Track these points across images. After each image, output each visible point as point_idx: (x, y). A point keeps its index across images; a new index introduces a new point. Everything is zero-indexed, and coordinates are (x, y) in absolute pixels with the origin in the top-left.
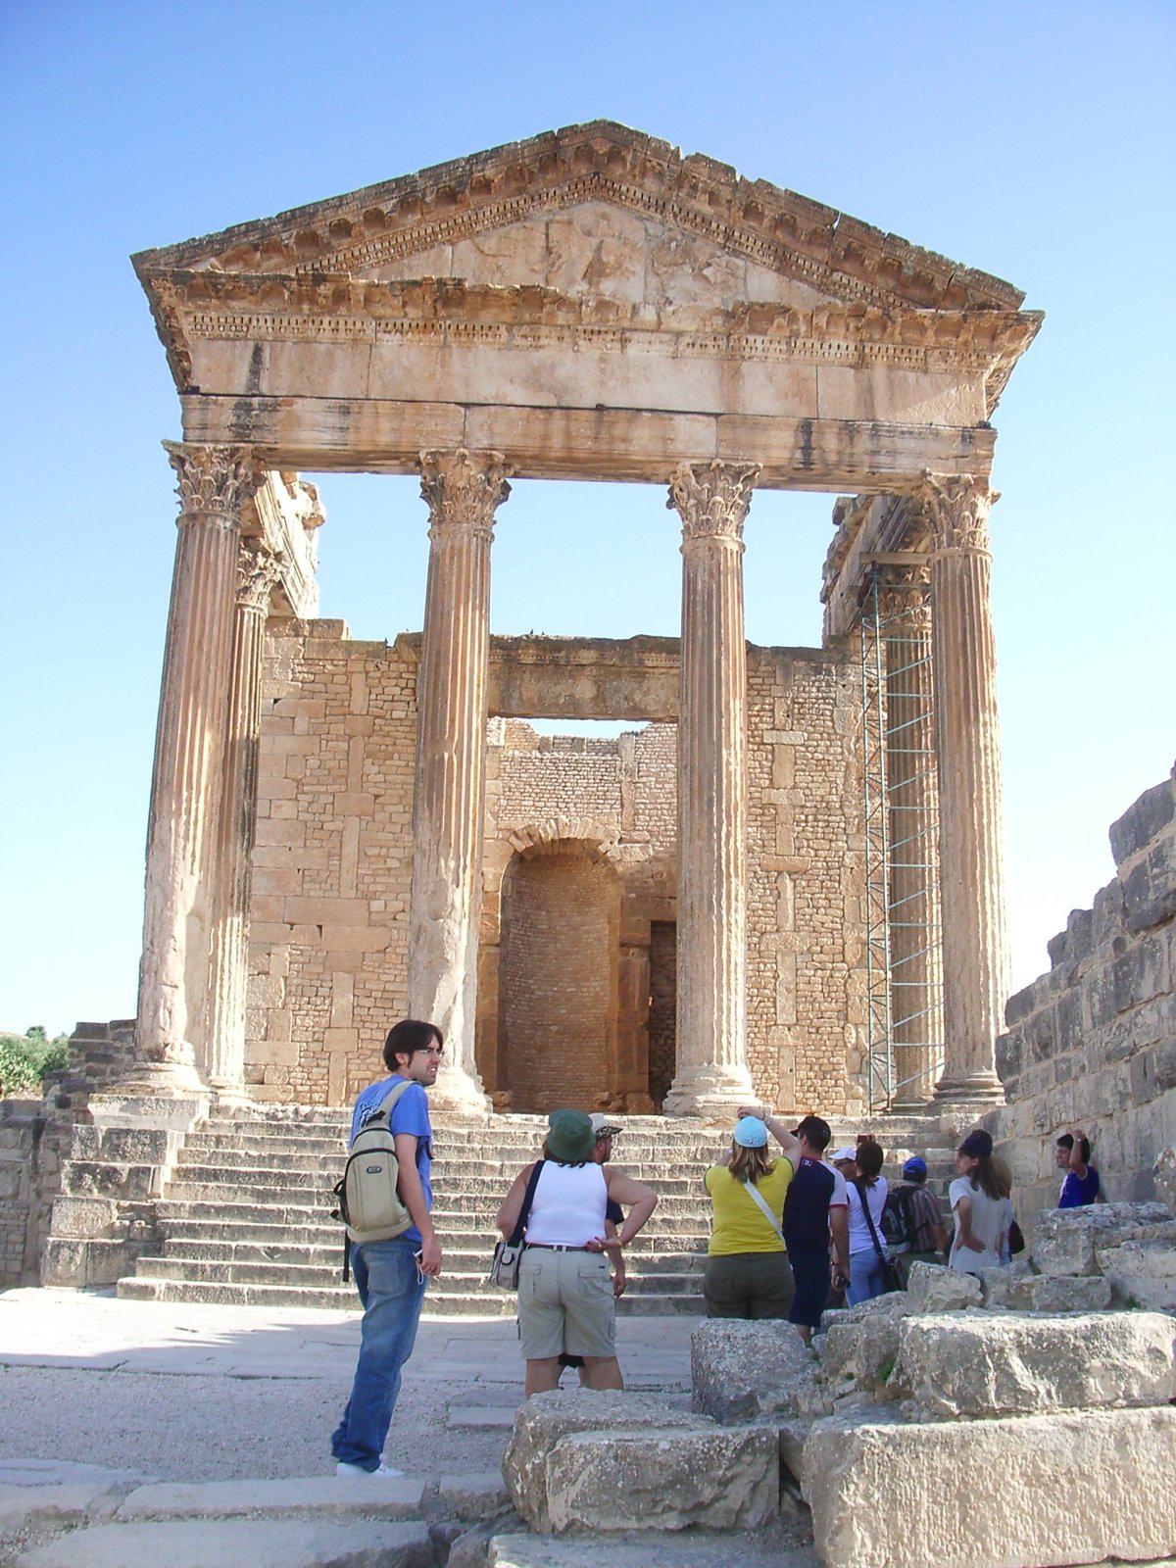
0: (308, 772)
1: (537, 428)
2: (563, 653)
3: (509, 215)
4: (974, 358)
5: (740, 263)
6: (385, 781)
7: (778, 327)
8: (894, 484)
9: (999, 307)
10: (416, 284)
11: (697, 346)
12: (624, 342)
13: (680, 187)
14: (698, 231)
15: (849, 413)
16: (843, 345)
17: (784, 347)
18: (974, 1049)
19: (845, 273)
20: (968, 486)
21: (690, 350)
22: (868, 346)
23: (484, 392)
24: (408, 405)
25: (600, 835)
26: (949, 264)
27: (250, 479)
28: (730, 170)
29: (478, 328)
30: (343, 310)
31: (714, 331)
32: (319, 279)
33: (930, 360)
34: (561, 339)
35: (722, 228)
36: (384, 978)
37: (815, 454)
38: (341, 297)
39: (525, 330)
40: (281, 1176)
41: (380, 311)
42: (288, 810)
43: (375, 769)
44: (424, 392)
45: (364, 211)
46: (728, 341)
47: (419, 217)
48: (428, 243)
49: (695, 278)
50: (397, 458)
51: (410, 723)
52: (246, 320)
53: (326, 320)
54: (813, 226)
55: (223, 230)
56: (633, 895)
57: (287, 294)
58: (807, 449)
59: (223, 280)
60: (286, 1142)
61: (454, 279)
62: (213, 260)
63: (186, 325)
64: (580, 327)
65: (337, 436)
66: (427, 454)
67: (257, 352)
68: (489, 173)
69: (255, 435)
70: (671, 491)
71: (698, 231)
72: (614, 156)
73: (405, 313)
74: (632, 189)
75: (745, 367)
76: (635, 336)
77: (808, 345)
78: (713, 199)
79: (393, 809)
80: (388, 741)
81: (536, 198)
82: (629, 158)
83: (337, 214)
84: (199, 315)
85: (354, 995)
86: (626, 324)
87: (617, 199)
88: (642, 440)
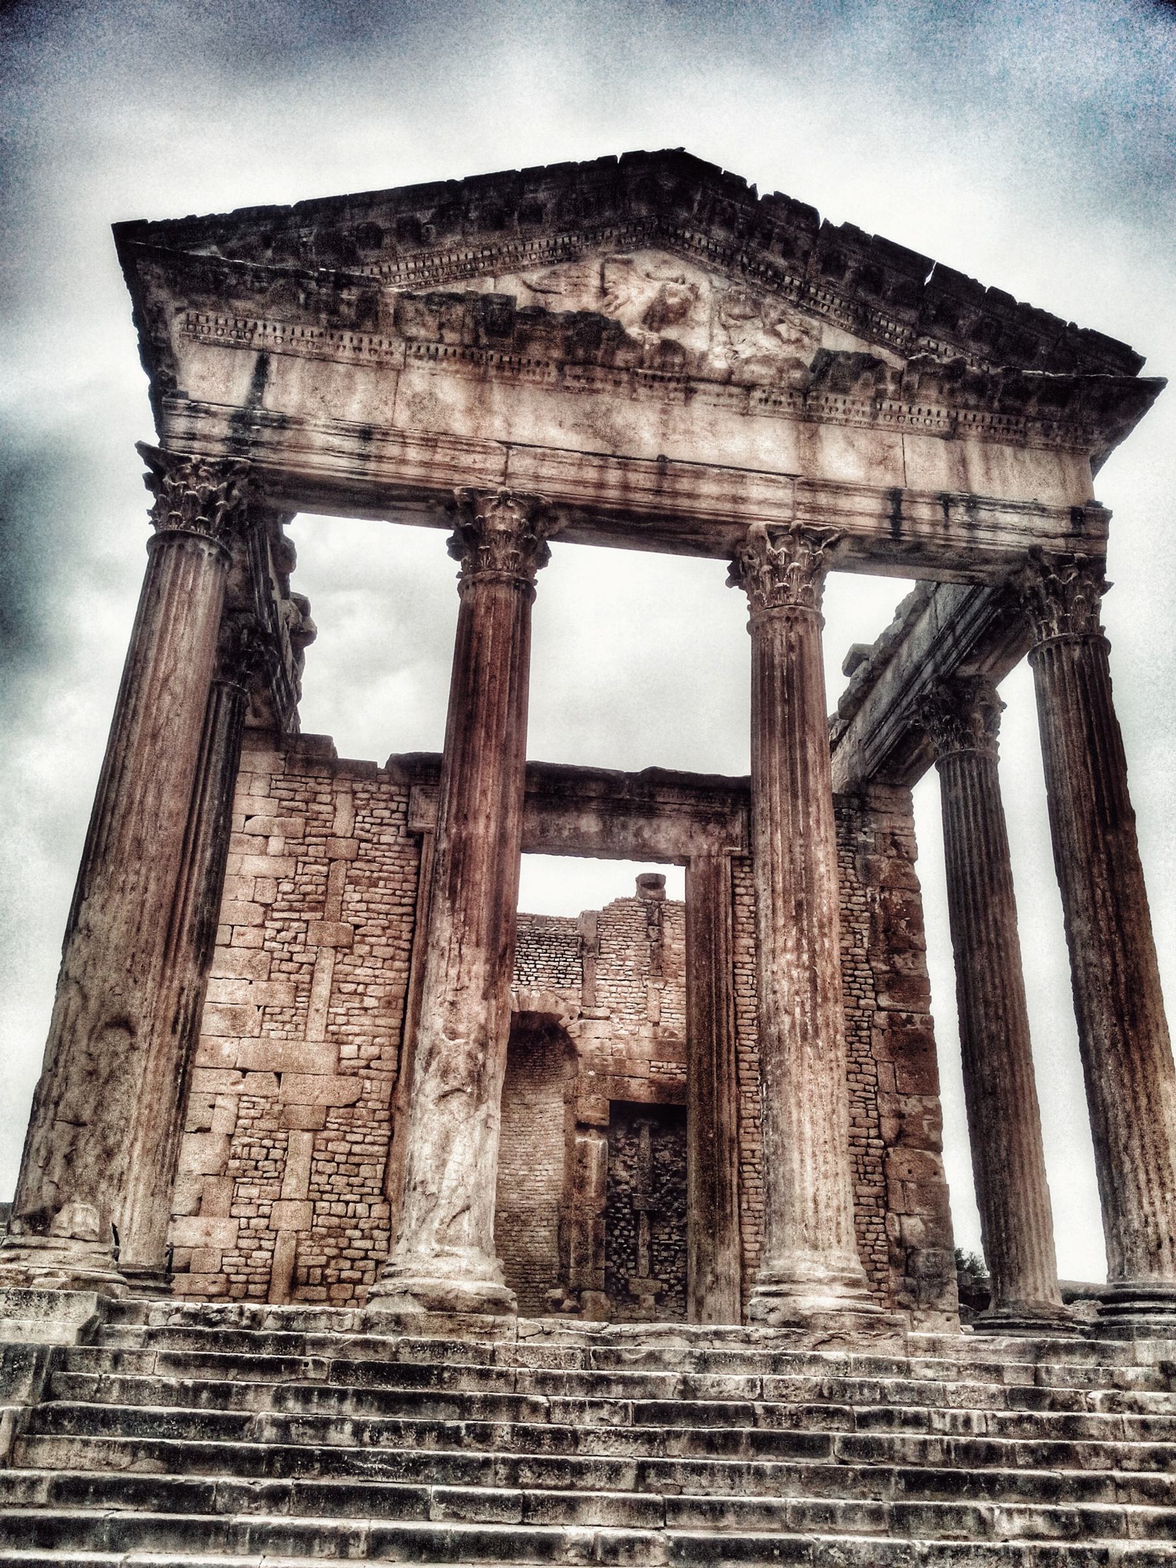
0: (280, 896)
2: (569, 784)
4: (1080, 433)
5: (815, 323)
6: (368, 910)
8: (989, 568)
9: (1112, 373)
12: (689, 393)
13: (752, 236)
16: (934, 410)
17: (867, 409)
18: (1159, 1246)
19: (934, 337)
20: (1082, 565)
21: (762, 406)
22: (962, 413)
23: (524, 431)
24: (443, 438)
25: (561, 1009)
26: (1059, 323)
27: (244, 507)
28: (810, 213)
29: (524, 361)
30: (369, 325)
31: (790, 386)
32: (344, 282)
33: (1031, 434)
34: (617, 383)
35: (797, 283)
36: (349, 1137)
37: (906, 526)
39: (579, 371)
40: (211, 1421)
42: (252, 936)
43: (357, 896)
46: (805, 400)
47: (458, 237)
48: (468, 272)
49: (766, 332)
50: (425, 499)
51: (397, 848)
52: (250, 324)
53: (347, 335)
54: (902, 279)
55: (229, 211)
56: (592, 1073)
57: (302, 297)
58: (896, 518)
59: (226, 270)
60: (225, 1364)
62: (214, 248)
63: (176, 325)
67: (262, 368)
68: (542, 196)
69: (254, 452)
70: (730, 569)
72: (682, 197)
73: (442, 337)
74: (697, 236)
75: (823, 429)
77: (895, 408)
79: (373, 940)
80: (374, 867)
81: (593, 236)
83: (366, 215)
84: (193, 312)
85: (313, 1159)
86: (693, 372)
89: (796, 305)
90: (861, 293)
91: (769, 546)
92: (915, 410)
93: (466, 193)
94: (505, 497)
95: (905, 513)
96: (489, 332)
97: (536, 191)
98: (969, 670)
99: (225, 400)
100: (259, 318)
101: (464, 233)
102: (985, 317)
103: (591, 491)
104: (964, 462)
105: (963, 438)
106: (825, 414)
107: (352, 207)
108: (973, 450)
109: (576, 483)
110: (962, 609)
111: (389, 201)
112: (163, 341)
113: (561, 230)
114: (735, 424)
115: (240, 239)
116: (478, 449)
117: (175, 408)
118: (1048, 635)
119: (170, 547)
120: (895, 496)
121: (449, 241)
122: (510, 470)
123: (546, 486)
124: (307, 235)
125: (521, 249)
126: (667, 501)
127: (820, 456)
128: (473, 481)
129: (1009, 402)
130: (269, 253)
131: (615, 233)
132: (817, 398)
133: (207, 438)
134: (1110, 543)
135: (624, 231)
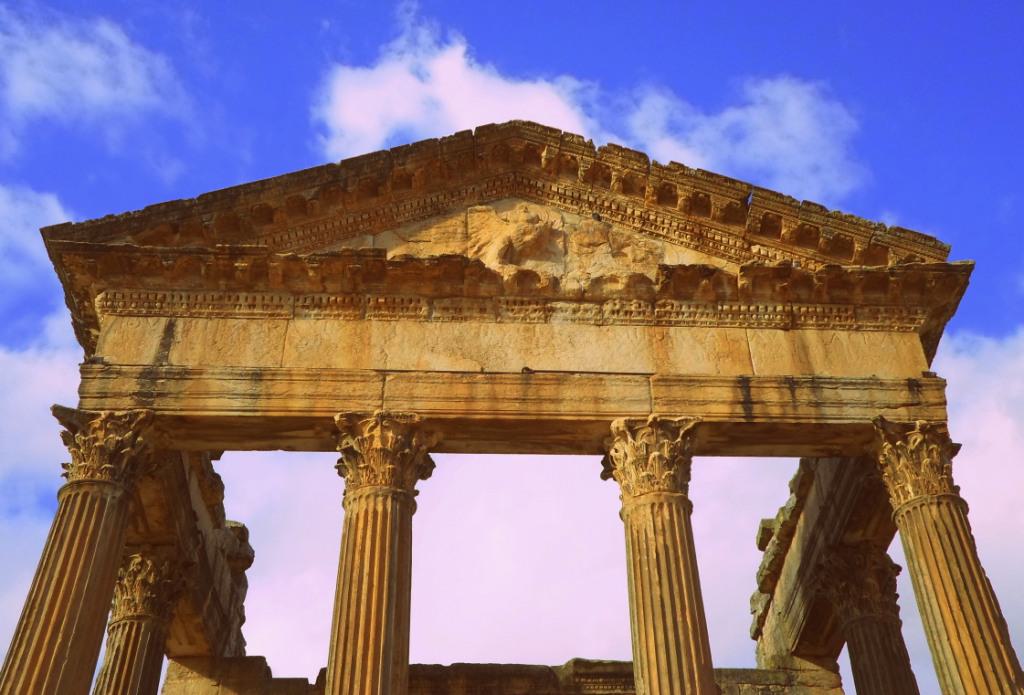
1: (461, 390)
3: (429, 209)
4: (905, 315)
7: (705, 291)
10: (335, 256)
11: (621, 313)
14: (614, 218)
15: (786, 368)
16: (770, 309)
20: (923, 429)
30: (261, 285)
34: (483, 310)
35: (637, 213)
37: (757, 409)
38: (260, 272)
39: (447, 302)
41: (299, 285)
44: (342, 362)
45: (286, 197)
46: (653, 308)
47: (340, 207)
49: (614, 256)
53: (243, 295)
54: (728, 201)
58: (748, 403)
61: (374, 250)
62: (129, 238)
64: (502, 298)
65: (248, 403)
66: (341, 416)
67: (170, 330)
68: (410, 167)
69: (158, 403)
70: (604, 463)
71: (614, 218)
75: (672, 329)
76: (559, 305)
78: (628, 186)
82: (544, 154)
86: (549, 294)
87: (535, 195)
88: (571, 404)
89: (641, 231)
90: (694, 217)
91: (630, 439)
92: (752, 308)
93: (343, 172)
94: (382, 417)
95: (755, 398)
96: (365, 280)
97: (403, 164)
98: (857, 536)
99: (135, 361)
100: (168, 290)
101: (344, 204)
102: (804, 225)
103: (462, 406)
104: (805, 348)
105: (802, 326)
106: (673, 319)
107: (246, 194)
108: (811, 335)
109: (448, 399)
110: (837, 479)
111: (278, 184)
112: (91, 317)
113: (430, 192)
114: (590, 333)
115: (152, 229)
116: (358, 378)
117: (91, 372)
118: (905, 498)
119: (76, 495)
120: (744, 383)
121: (333, 210)
122: (385, 395)
123: (420, 405)
124: (210, 220)
125: (395, 210)
126: (532, 408)
127: (671, 355)
128: (353, 407)
129: (836, 293)
130: (177, 237)
131: (477, 189)
132: (664, 305)
133: (118, 395)
134: (948, 407)
135: (486, 185)
